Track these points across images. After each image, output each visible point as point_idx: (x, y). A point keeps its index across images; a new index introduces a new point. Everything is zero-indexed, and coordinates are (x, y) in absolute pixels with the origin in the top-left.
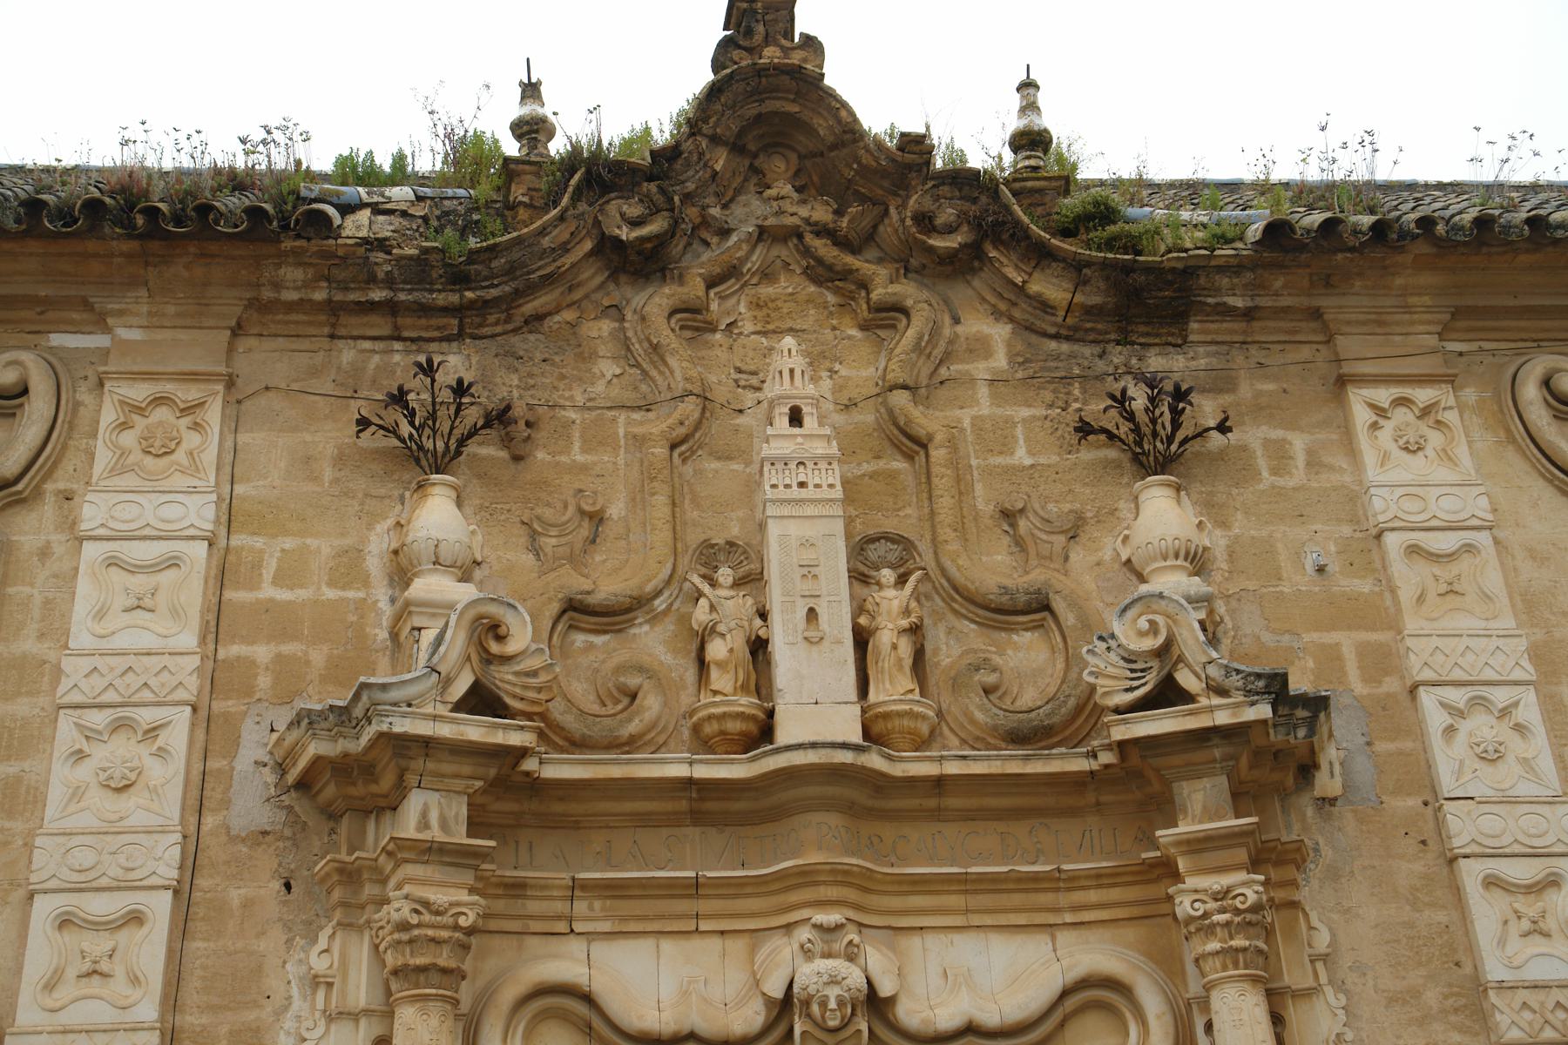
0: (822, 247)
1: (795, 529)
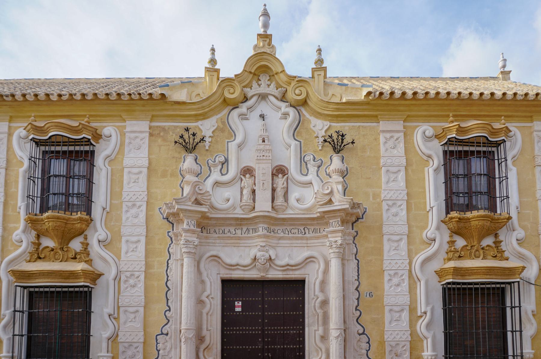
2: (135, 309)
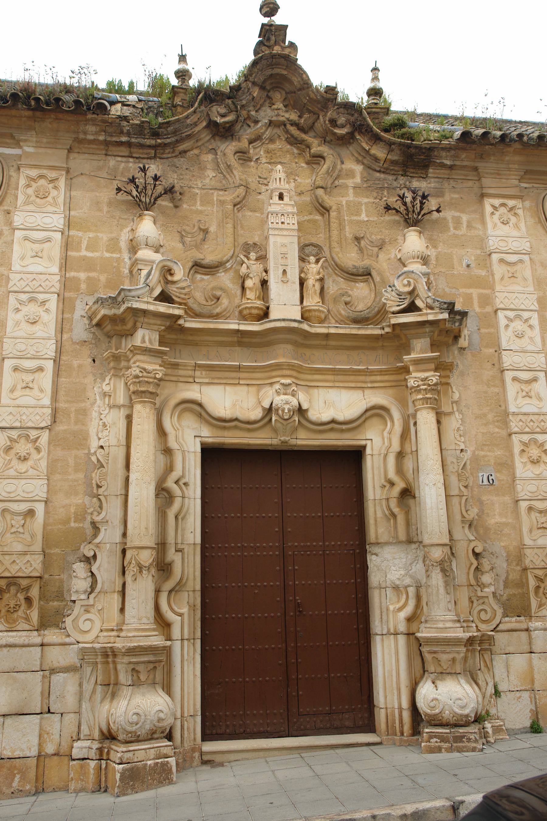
0: (293, 130)
1: (279, 240)
2: (23, 507)
